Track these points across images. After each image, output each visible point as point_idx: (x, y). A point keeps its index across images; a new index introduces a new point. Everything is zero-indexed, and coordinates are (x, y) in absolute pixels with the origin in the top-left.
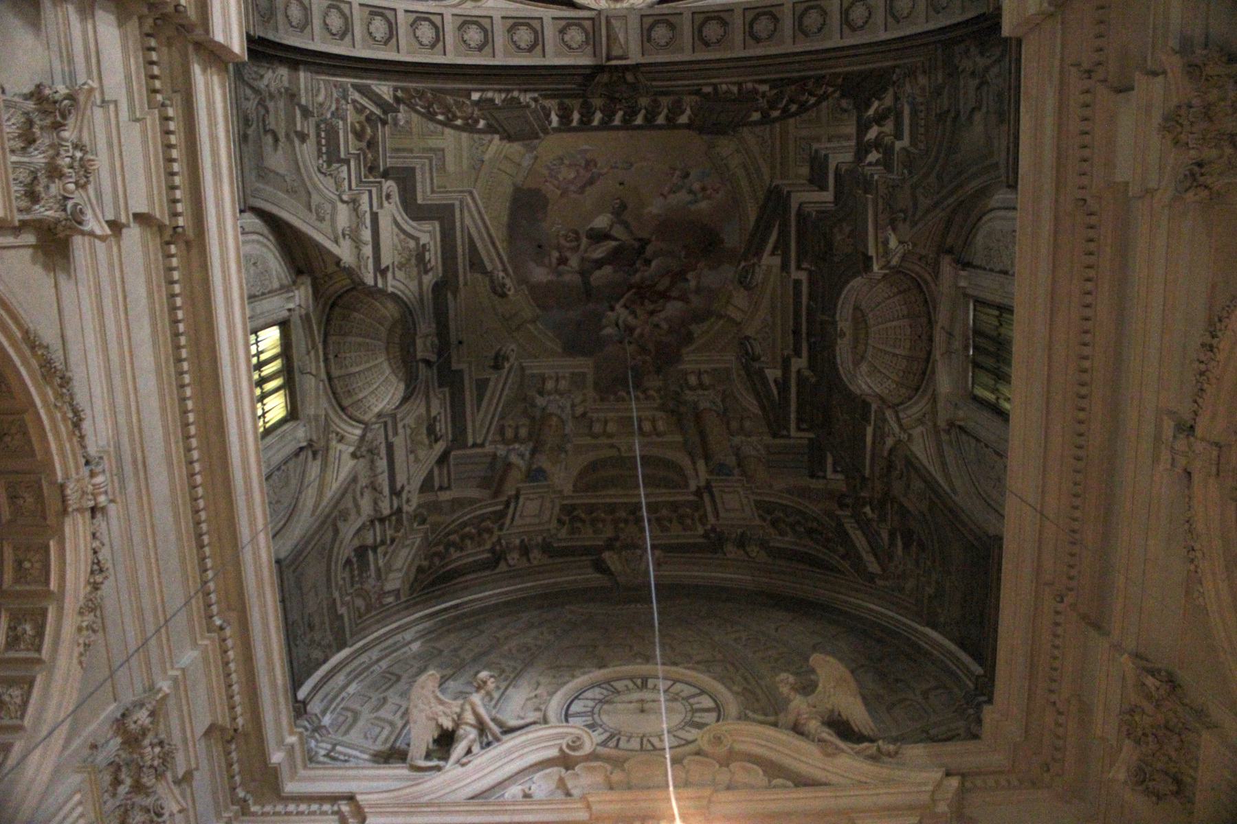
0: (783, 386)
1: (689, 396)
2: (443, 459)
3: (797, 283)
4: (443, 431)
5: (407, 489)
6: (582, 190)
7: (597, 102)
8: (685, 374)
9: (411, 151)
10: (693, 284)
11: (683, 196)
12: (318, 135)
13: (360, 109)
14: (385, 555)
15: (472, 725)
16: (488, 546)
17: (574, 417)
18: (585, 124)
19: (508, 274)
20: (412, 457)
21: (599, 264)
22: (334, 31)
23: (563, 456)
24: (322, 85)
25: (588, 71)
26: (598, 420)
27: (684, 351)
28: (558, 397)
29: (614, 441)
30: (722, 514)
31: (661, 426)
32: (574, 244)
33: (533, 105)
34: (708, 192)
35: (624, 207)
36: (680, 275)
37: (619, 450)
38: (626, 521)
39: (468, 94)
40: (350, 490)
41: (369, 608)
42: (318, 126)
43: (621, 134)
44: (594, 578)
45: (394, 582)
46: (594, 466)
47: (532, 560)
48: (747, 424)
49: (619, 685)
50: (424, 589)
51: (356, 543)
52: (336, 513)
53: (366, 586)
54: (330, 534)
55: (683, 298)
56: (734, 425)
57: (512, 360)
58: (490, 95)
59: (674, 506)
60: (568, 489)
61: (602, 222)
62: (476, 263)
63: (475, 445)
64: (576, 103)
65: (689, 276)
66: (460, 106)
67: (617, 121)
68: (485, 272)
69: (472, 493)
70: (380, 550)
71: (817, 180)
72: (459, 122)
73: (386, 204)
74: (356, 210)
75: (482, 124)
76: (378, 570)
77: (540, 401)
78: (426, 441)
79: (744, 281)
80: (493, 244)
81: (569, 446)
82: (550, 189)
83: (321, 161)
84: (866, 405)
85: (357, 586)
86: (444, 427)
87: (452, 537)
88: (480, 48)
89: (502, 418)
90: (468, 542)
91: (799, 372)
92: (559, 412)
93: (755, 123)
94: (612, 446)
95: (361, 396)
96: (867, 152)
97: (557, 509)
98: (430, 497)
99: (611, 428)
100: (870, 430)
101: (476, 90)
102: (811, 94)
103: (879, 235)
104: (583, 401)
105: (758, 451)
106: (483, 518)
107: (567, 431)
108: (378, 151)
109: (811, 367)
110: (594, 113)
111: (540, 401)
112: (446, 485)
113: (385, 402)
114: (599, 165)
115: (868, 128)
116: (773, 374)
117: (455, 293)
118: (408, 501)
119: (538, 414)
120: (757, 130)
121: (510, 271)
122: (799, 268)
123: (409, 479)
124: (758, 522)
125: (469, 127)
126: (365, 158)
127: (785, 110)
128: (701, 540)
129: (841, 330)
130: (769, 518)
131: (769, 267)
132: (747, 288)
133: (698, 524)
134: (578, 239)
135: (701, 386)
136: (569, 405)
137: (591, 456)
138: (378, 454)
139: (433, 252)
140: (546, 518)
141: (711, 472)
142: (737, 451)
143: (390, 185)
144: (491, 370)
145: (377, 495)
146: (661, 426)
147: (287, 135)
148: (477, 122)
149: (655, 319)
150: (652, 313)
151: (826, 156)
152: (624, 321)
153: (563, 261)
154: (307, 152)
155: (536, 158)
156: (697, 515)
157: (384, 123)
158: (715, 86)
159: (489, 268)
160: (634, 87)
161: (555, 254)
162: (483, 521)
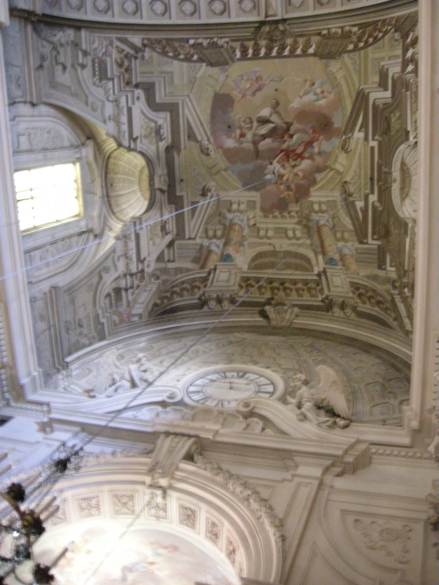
0: (365, 211)
1: (315, 217)
2: (171, 245)
3: (372, 148)
4: (171, 229)
5: (147, 259)
6: (254, 94)
7: (263, 43)
8: (312, 203)
9: (152, 73)
10: (316, 150)
11: (310, 97)
12: (94, 66)
13: (121, 51)
14: (133, 294)
15: (128, 381)
16: (197, 296)
17: (249, 227)
18: (256, 56)
19: (210, 143)
20: (151, 242)
21: (264, 137)
22: (100, 9)
23: (242, 248)
24: (96, 39)
25: (257, 25)
26: (262, 228)
27: (312, 189)
28: (239, 214)
29: (271, 241)
30: (332, 289)
31: (298, 234)
32: (249, 126)
33: (226, 45)
34: (326, 94)
35: (277, 104)
36: (309, 144)
37: (274, 247)
38: (278, 289)
39: (187, 40)
40: (111, 257)
41: (122, 321)
42: (93, 61)
43: (277, 60)
44: (259, 319)
45: (138, 309)
46: (260, 255)
47: (223, 307)
48: (346, 235)
49: (229, 374)
50: (158, 315)
51: (114, 285)
52: (101, 268)
53: (120, 310)
54: (95, 279)
55: (311, 158)
56: (339, 235)
57: (212, 192)
58: (200, 41)
59: (306, 282)
60: (245, 268)
61: (265, 112)
62: (191, 136)
63: (190, 239)
64: (251, 44)
65: (315, 144)
66: (183, 47)
67: (274, 53)
68: (197, 141)
69: (189, 265)
70: (130, 291)
71: (383, 85)
72: (182, 57)
73: (136, 102)
74: (118, 106)
75: (195, 57)
76: (128, 302)
77: (230, 216)
78: (160, 234)
79: (344, 148)
80: (202, 125)
81: (246, 243)
82: (236, 94)
83: (95, 79)
84: (406, 225)
85: (114, 309)
86: (171, 227)
87: (175, 289)
88: (192, 14)
89: (207, 223)
90: (185, 293)
91: (373, 203)
92: (240, 222)
93: (351, 51)
94: (270, 244)
95: (124, 207)
96: (407, 65)
97: (238, 279)
98: (162, 265)
99: (270, 233)
100: (408, 240)
101: (193, 38)
102: (380, 31)
103: (413, 118)
104: (254, 217)
105: (351, 251)
106: (194, 280)
107: (245, 234)
108: (132, 74)
109: (380, 199)
110: (261, 49)
111: (230, 216)
112: (172, 259)
113: (137, 210)
114: (264, 79)
115: (408, 50)
116: (360, 204)
117: (179, 154)
118: (148, 266)
119: (227, 223)
120: (352, 54)
121: (212, 140)
122: (373, 139)
123: (149, 255)
124: (351, 295)
125: (188, 59)
126: (124, 77)
127: (366, 42)
128: (321, 304)
129: (394, 178)
130: (357, 292)
131: (358, 139)
132: (346, 152)
133: (318, 293)
134: (251, 122)
135: (321, 211)
136: (245, 219)
137: (259, 249)
138: (130, 238)
139: (165, 129)
140: (232, 283)
141: (326, 263)
142: (340, 251)
143: (139, 92)
144: (200, 197)
145: (129, 261)
146: (298, 234)
147: (73, 66)
148: (192, 56)
149: (295, 170)
150: (294, 166)
151: (387, 69)
152: (278, 170)
153: (243, 135)
154: (86, 74)
155: (227, 76)
156: (318, 288)
157: (136, 58)
158: (329, 29)
159: (199, 138)
160: (283, 32)
161: (238, 132)
162: (194, 281)
